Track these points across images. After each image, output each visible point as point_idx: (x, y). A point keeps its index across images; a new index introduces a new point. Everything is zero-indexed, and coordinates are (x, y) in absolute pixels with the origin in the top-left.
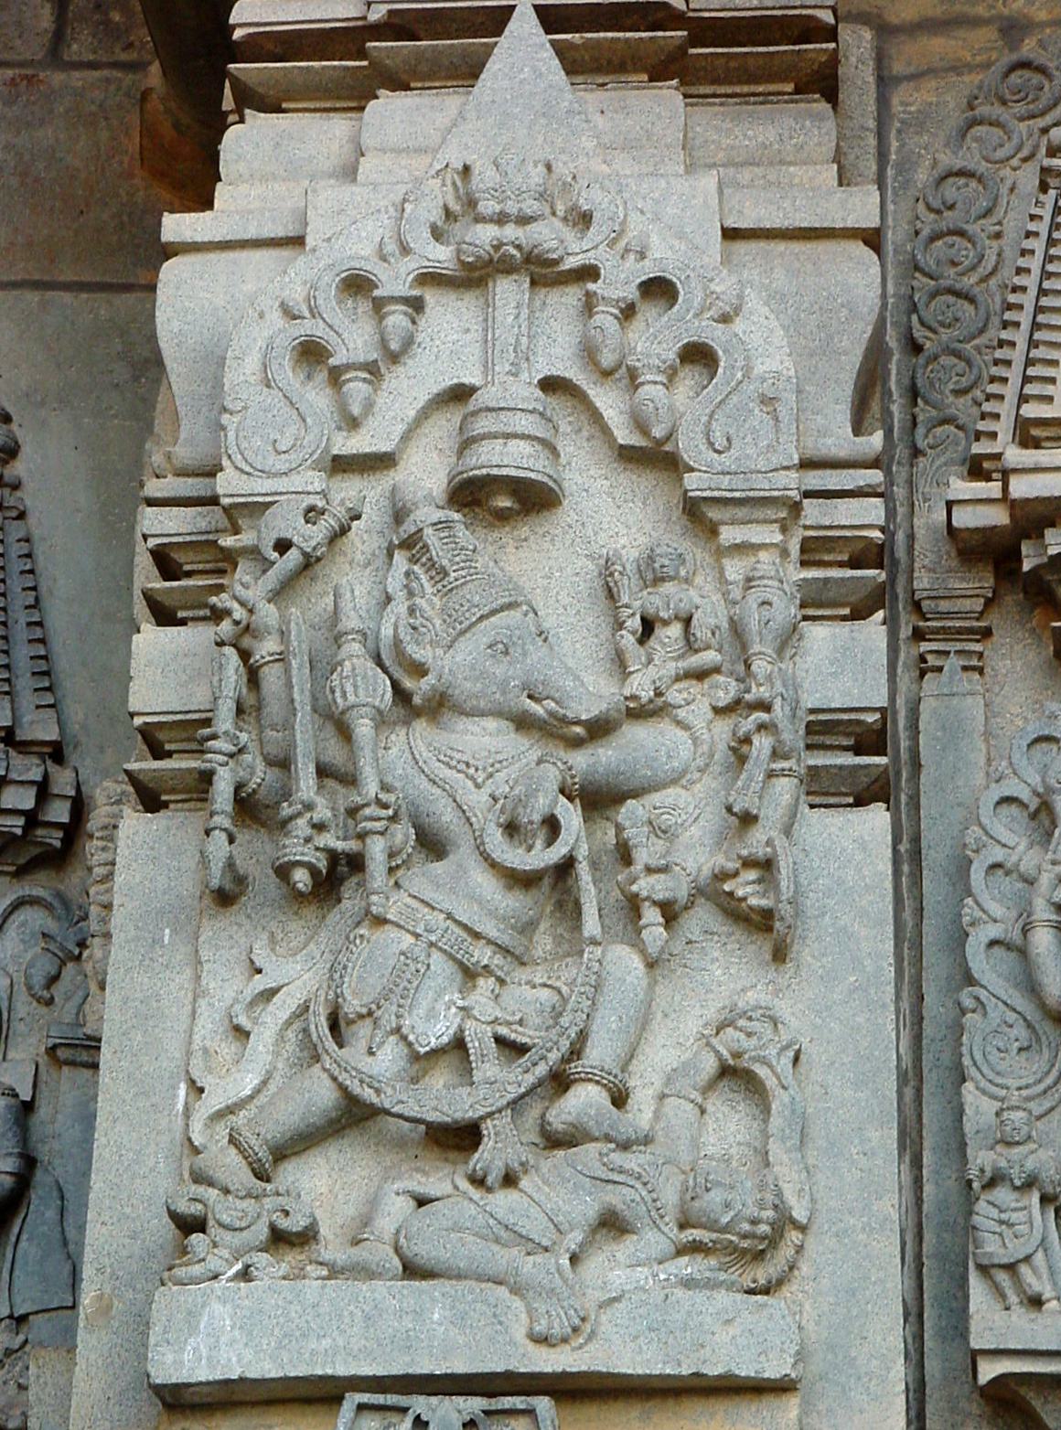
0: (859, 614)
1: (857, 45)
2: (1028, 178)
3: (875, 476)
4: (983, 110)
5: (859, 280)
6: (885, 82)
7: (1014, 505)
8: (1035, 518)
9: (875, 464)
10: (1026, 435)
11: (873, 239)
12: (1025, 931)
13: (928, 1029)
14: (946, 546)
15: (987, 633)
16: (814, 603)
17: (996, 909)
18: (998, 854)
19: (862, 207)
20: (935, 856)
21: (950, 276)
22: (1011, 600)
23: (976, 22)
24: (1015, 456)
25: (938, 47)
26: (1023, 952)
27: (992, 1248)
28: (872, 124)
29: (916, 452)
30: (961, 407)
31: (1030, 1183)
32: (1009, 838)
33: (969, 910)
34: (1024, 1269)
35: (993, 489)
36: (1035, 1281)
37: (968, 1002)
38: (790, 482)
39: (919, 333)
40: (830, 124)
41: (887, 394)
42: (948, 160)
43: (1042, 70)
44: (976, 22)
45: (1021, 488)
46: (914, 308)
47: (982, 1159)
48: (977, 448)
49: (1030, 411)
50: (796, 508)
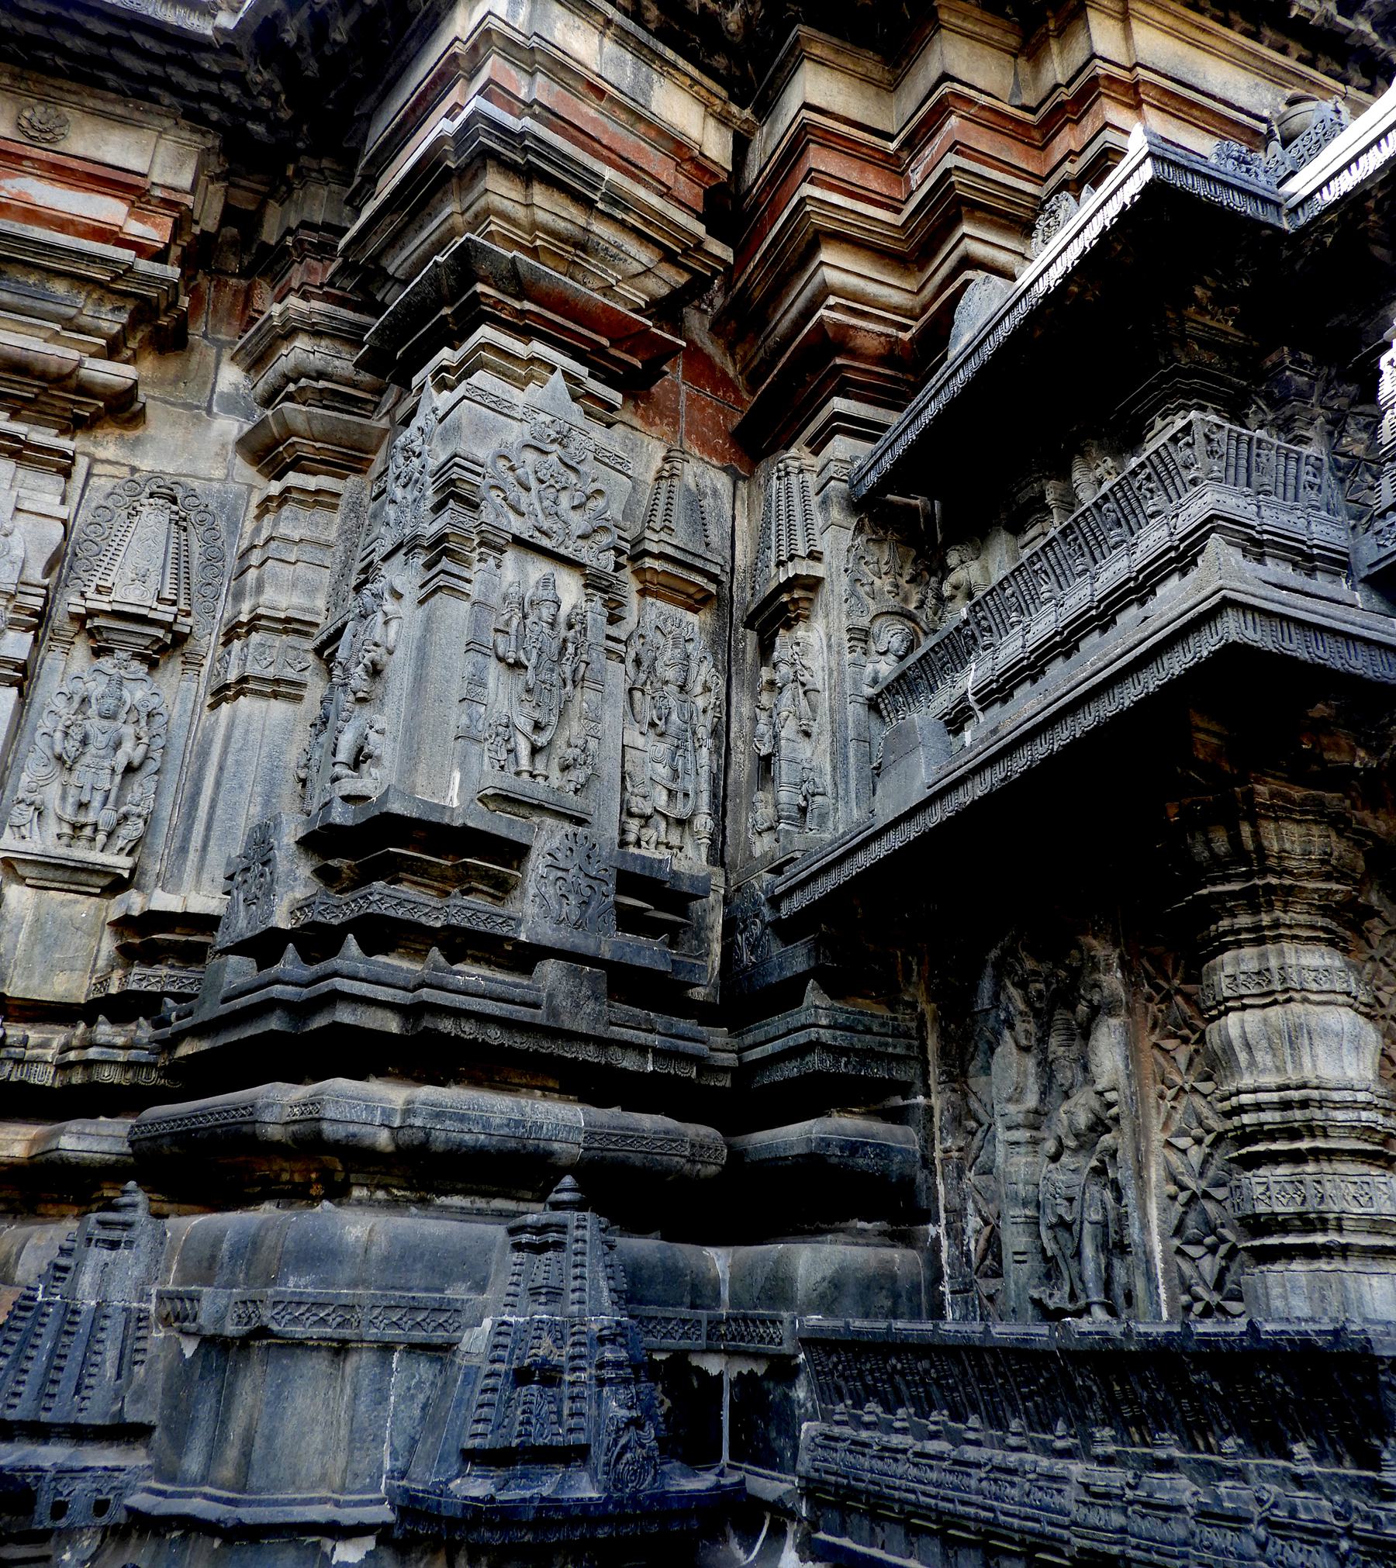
0: (27, 631)
1: (82, 463)
2: (124, 514)
6: (89, 475)
8: (92, 614)
16: (13, 624)
19: (64, 512)
22: (84, 635)
32: (60, 704)
36: (24, 831)
38: (12, 589)
50: (13, 596)
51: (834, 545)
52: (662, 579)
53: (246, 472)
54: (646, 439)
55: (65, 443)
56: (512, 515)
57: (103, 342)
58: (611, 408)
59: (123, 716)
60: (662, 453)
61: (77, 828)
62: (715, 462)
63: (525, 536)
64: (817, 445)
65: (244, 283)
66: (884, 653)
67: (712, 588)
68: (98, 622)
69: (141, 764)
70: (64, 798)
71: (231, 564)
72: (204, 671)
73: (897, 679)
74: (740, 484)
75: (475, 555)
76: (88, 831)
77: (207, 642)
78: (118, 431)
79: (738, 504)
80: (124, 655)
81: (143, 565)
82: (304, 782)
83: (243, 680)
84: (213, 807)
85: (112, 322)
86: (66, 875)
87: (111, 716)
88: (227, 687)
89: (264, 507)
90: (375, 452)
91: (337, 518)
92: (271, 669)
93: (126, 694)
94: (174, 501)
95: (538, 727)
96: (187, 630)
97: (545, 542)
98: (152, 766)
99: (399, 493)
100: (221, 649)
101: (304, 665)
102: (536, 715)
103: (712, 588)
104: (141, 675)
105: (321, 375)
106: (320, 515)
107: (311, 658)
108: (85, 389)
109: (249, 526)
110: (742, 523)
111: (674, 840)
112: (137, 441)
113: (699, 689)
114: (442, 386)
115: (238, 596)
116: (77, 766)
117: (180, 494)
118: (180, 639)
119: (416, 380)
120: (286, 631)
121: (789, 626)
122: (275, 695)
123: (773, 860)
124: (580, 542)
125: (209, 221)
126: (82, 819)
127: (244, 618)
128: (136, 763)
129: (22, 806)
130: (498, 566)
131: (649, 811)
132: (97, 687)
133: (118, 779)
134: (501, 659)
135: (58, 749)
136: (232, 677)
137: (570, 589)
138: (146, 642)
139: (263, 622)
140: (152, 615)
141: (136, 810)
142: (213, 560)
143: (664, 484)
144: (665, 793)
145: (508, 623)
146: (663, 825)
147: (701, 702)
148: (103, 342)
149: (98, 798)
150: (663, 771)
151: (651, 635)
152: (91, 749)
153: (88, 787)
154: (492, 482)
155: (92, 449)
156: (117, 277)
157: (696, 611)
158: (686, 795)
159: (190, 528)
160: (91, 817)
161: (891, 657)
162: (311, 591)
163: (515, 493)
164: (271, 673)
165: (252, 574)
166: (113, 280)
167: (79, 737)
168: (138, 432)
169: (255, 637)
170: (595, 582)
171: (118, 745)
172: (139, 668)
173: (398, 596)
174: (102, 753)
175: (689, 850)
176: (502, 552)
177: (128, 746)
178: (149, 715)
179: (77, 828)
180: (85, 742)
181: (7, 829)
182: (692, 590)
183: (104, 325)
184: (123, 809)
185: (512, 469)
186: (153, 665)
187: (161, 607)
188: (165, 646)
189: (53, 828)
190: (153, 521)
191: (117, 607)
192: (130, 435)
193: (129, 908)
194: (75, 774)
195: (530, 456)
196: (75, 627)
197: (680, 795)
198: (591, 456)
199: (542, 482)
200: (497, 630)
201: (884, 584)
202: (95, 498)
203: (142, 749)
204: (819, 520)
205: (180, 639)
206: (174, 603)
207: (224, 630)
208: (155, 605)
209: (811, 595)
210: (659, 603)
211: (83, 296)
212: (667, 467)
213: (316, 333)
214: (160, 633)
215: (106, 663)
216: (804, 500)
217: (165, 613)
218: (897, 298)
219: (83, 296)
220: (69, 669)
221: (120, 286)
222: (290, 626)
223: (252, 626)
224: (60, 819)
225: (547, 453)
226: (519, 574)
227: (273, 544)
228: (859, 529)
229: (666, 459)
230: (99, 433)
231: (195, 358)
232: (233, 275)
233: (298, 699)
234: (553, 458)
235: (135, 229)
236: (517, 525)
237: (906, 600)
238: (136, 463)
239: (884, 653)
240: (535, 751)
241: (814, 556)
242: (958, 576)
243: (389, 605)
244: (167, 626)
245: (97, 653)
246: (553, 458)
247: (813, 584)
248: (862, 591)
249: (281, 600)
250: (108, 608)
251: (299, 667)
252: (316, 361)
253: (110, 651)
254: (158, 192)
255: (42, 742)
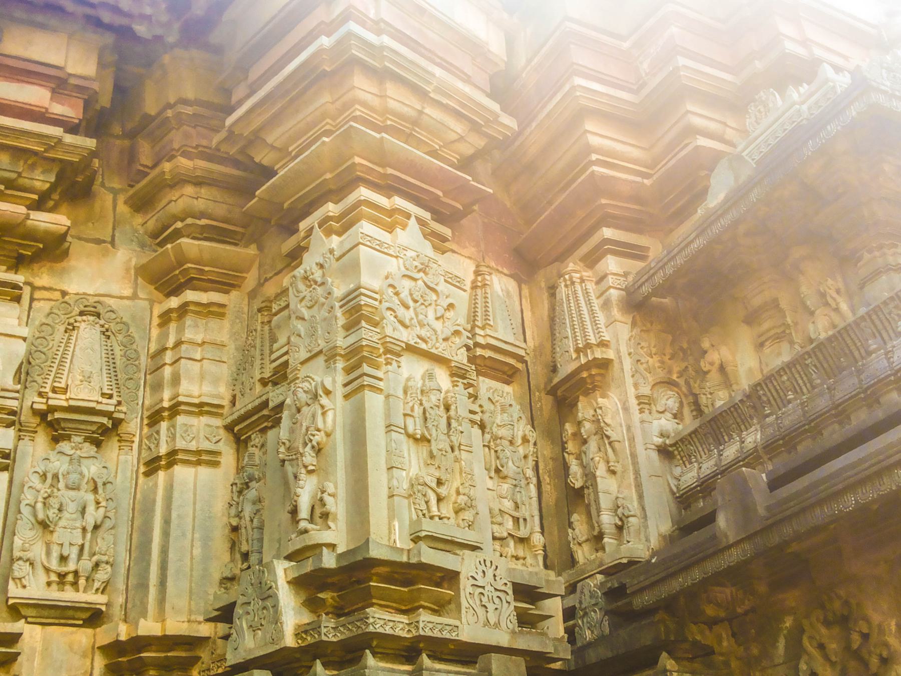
0: (8, 426)
1: (27, 290)
2: (62, 328)
3: (17, 395)
4: (55, 311)
5: (21, 349)
6: (32, 300)
7: (48, 406)
8: (53, 409)
9: (18, 392)
10: (54, 390)
11: (25, 339)
12: (36, 503)
13: (8, 522)
14: (30, 412)
15: (36, 432)
17: (29, 497)
18: (31, 484)
19: (25, 332)
20: (16, 482)
21: (40, 348)
23: (56, 290)
24: (51, 395)
25: (46, 294)
26: (34, 507)
27: (17, 574)
28: (27, 308)
29: (26, 388)
30: (39, 379)
31: (28, 560)
32: (36, 481)
33: (23, 496)
34: (23, 580)
35: (44, 400)
37: (18, 517)
39: (31, 360)
40: (18, 310)
41: (21, 373)
42: (44, 320)
43: (69, 304)
44: (56, 290)
45: (51, 402)
46: (31, 354)
47: (17, 554)
48: (42, 390)
49: (56, 384)
51: (617, 337)
52: (488, 363)
53: (146, 291)
54: (462, 258)
55: (19, 278)
56: (401, 328)
57: (36, 197)
58: (444, 239)
59: (84, 486)
60: (473, 268)
61: (62, 576)
62: (505, 271)
63: (412, 342)
64: (592, 260)
65: (127, 143)
66: (662, 412)
67: (520, 366)
68: (57, 415)
69: (102, 522)
70: (48, 553)
71: (144, 361)
72: (135, 446)
73: (690, 435)
74: (523, 286)
75: (382, 360)
76: (70, 578)
77: (134, 426)
78: (48, 264)
79: (524, 300)
80: (77, 439)
81: (88, 368)
82: (235, 529)
83: (173, 453)
84: (164, 551)
85: (41, 180)
86: (58, 613)
87: (77, 488)
88: (158, 458)
89: (165, 318)
90: (247, 272)
91: (226, 323)
92: (194, 443)
93: (85, 471)
94: (98, 315)
95: (439, 483)
96: (122, 416)
97: (423, 346)
98: (108, 524)
99: (306, 313)
100: (146, 430)
101: (218, 438)
102: (437, 474)
103: (520, 366)
104: (92, 453)
105: (202, 215)
106: (214, 323)
107: (222, 433)
108: (32, 235)
109: (155, 332)
110: (528, 315)
111: (521, 553)
112: (63, 271)
113: (520, 441)
114: (329, 233)
115: (157, 387)
116: (57, 529)
117: (100, 309)
118: (117, 423)
119: (303, 225)
120: (201, 413)
121: (587, 393)
122: (199, 463)
123: (601, 565)
124: (445, 344)
125: (105, 101)
126: (64, 569)
127: (166, 404)
128: (98, 523)
129: (20, 562)
130: (399, 367)
131: (505, 534)
132: (59, 465)
133: (89, 535)
134: (409, 436)
135: (41, 516)
136: (163, 450)
137: (443, 379)
138: (94, 428)
139: (183, 407)
140: (99, 407)
141: (105, 558)
142: (131, 359)
143: (479, 291)
144: (511, 519)
145: (412, 409)
146: (512, 543)
147: (521, 451)
148: (36, 197)
149: (74, 552)
150: (508, 505)
151: (488, 406)
152: (66, 515)
153: (66, 544)
154: (388, 305)
155: (31, 280)
156: (50, 148)
157: (508, 383)
158: (525, 520)
159: (112, 337)
160: (71, 566)
161: (669, 415)
162: (216, 381)
163: (401, 311)
164: (193, 446)
165: (167, 371)
166: (46, 151)
167: (57, 506)
168: (64, 264)
169: (181, 419)
170: (458, 374)
171: (83, 511)
172: (89, 449)
173: (328, 393)
174: (74, 516)
175: (529, 560)
176: (399, 356)
177: (91, 508)
178: (104, 484)
179: (62, 576)
180: (60, 510)
181: (11, 582)
182: (506, 369)
183: (37, 184)
184: (95, 558)
185: (397, 294)
186: (98, 444)
187: (105, 401)
188: (105, 431)
189: (43, 578)
190: (88, 334)
191: (72, 403)
192: (58, 266)
193: (118, 635)
194: (55, 535)
195: (407, 283)
196: (37, 420)
197: (521, 521)
198: (442, 278)
199: (416, 301)
200: (405, 415)
201: (654, 361)
202: (39, 317)
203: (102, 511)
204: (601, 318)
205: (117, 423)
206: (110, 397)
207: (146, 414)
208: (100, 399)
209: (602, 371)
210: (487, 380)
211: (22, 163)
212: (479, 278)
213: (199, 182)
214: (104, 420)
215: (65, 446)
216: (589, 303)
217: (108, 406)
218: (635, 153)
219: (22, 163)
220: (36, 452)
221: (50, 155)
222: (202, 408)
223: (175, 410)
224: (47, 570)
225: (415, 280)
226: (412, 370)
227: (184, 347)
228: (634, 324)
229: (477, 273)
230: (36, 266)
231: (97, 205)
232: (117, 137)
233: (216, 464)
234: (420, 282)
235: (58, 109)
236: (405, 336)
237: (670, 372)
238: (65, 288)
239: (662, 412)
240: (440, 499)
241: (603, 344)
242: (714, 357)
243: (324, 400)
244: (108, 415)
245: (56, 440)
246: (420, 282)
247: (605, 364)
248: (642, 368)
249: (192, 389)
250: (65, 404)
251: (214, 440)
252: (200, 205)
253: (68, 438)
254: (72, 81)
255: (26, 511)
